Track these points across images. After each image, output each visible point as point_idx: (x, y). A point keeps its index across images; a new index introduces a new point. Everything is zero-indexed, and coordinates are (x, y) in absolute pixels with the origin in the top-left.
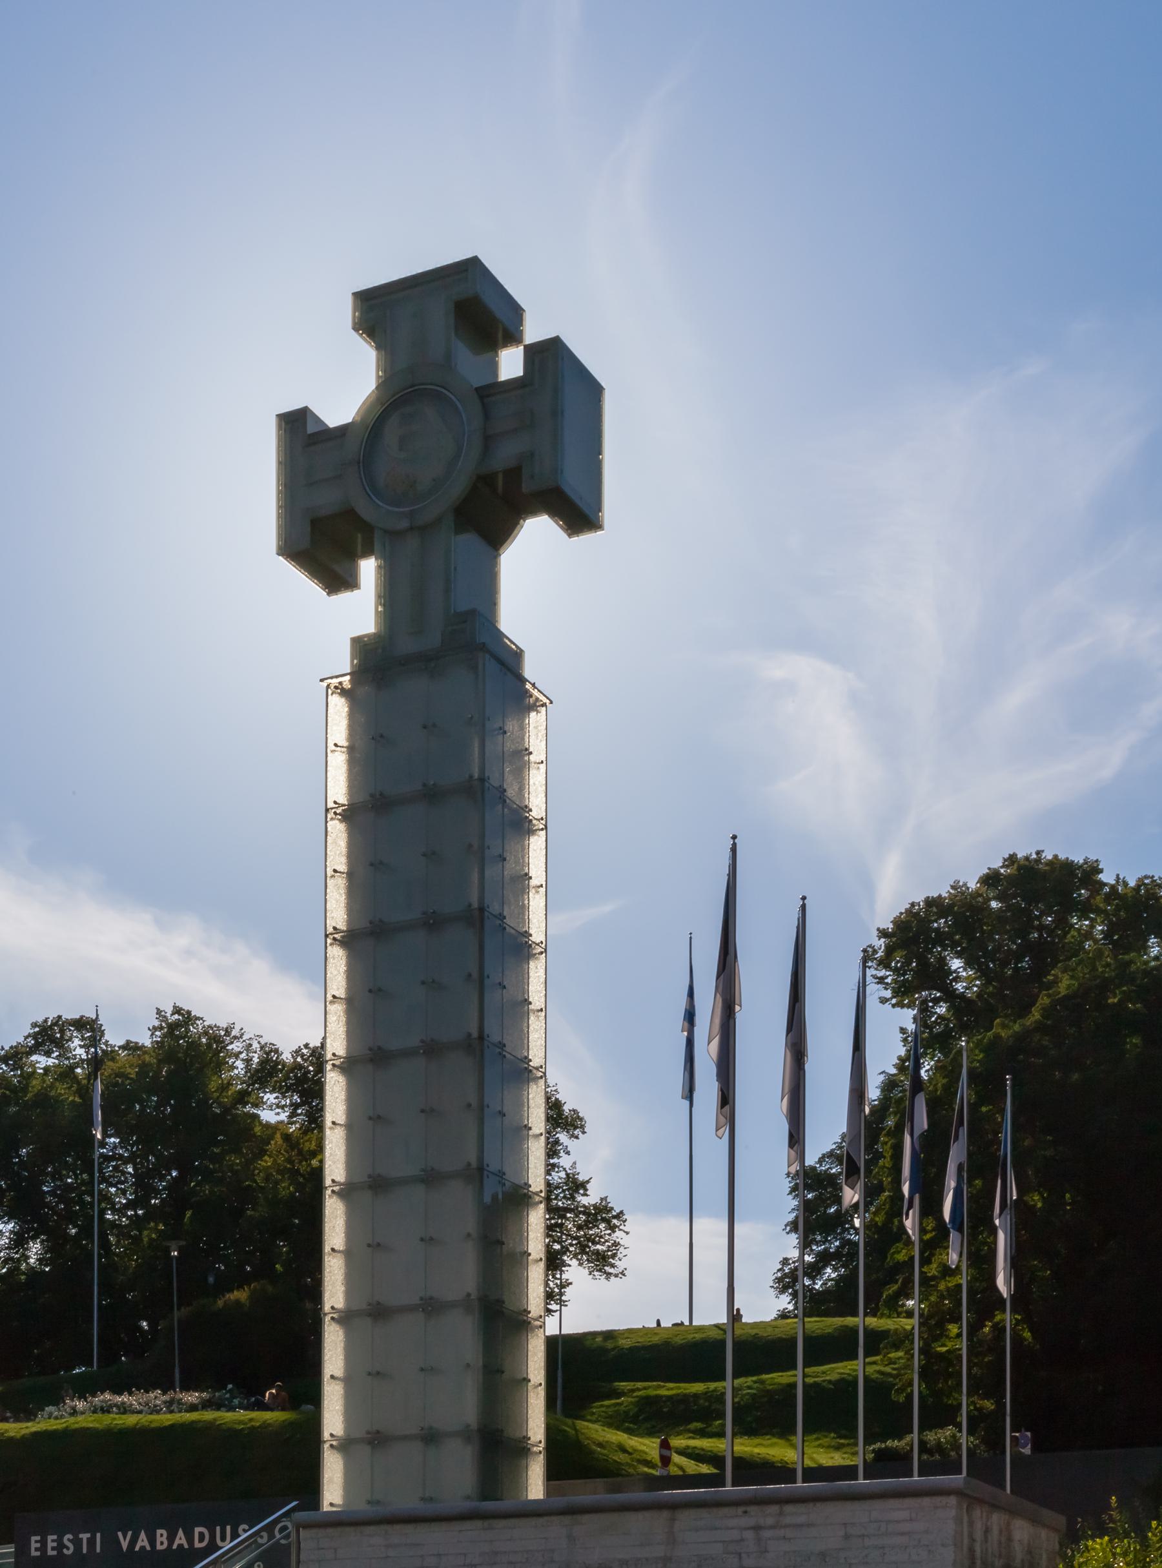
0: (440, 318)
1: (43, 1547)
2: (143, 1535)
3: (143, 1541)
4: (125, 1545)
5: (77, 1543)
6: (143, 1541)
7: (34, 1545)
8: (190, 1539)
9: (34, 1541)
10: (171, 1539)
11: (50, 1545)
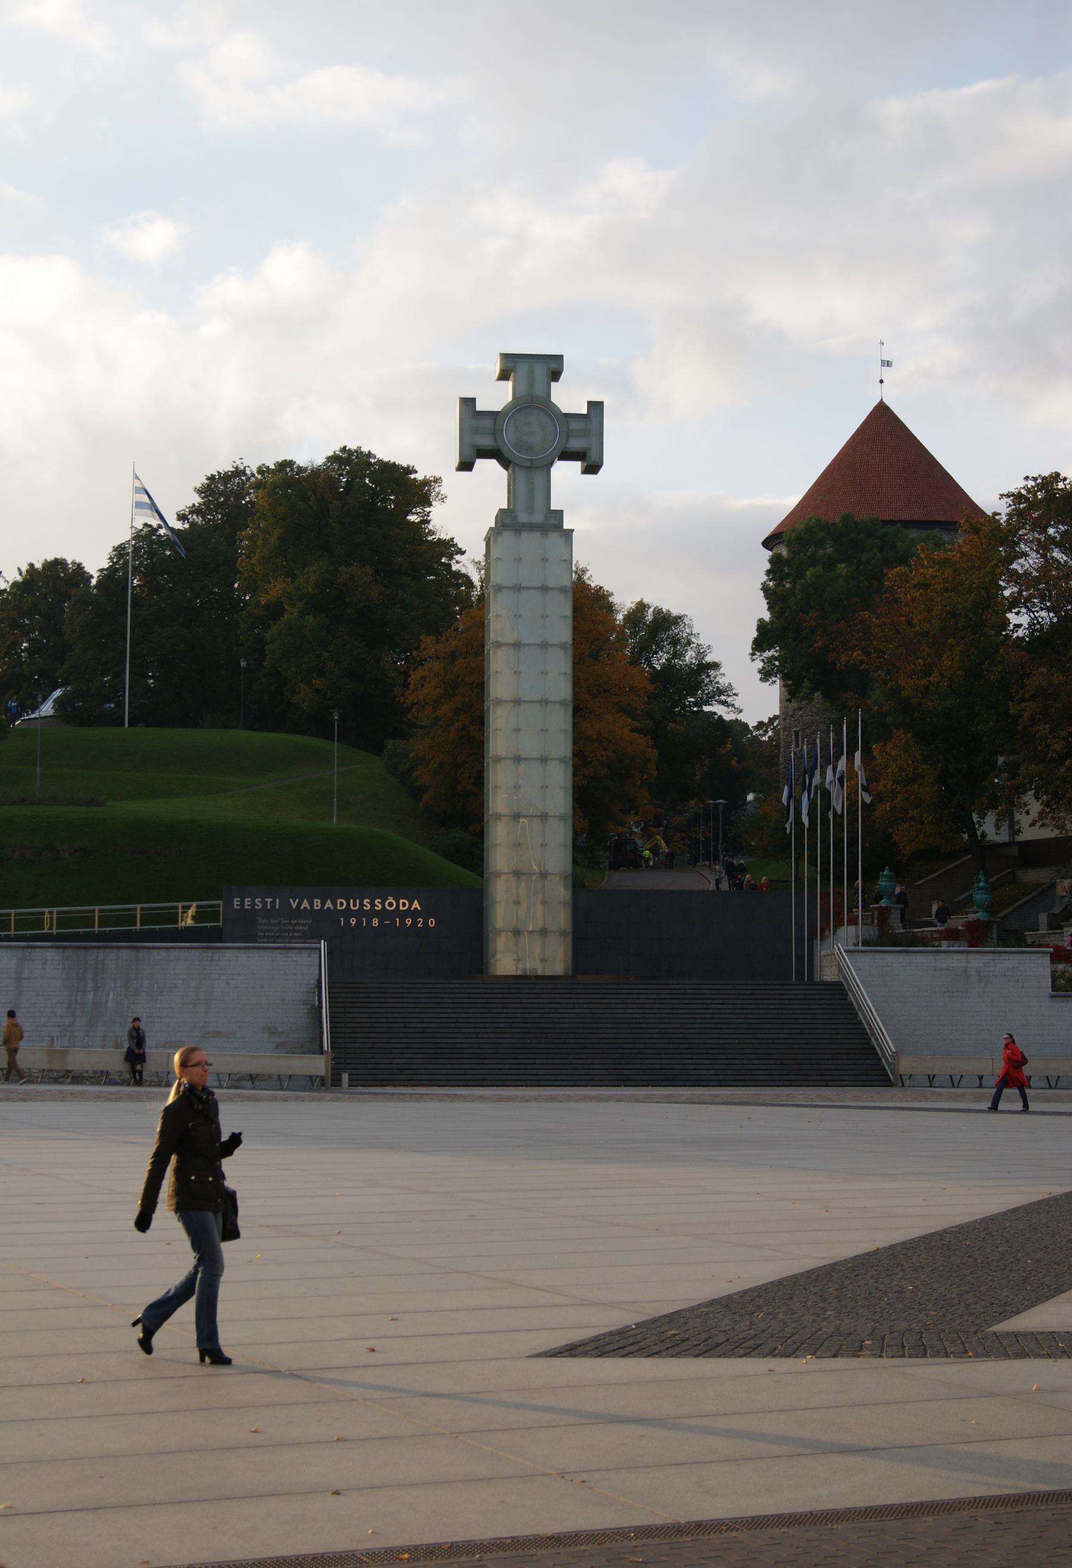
0: (533, 372)
1: (242, 904)
2: (305, 901)
3: (305, 904)
4: (294, 906)
5: (264, 903)
6: (305, 904)
7: (236, 903)
8: (334, 904)
9: (236, 901)
10: (323, 904)
11: (246, 903)
